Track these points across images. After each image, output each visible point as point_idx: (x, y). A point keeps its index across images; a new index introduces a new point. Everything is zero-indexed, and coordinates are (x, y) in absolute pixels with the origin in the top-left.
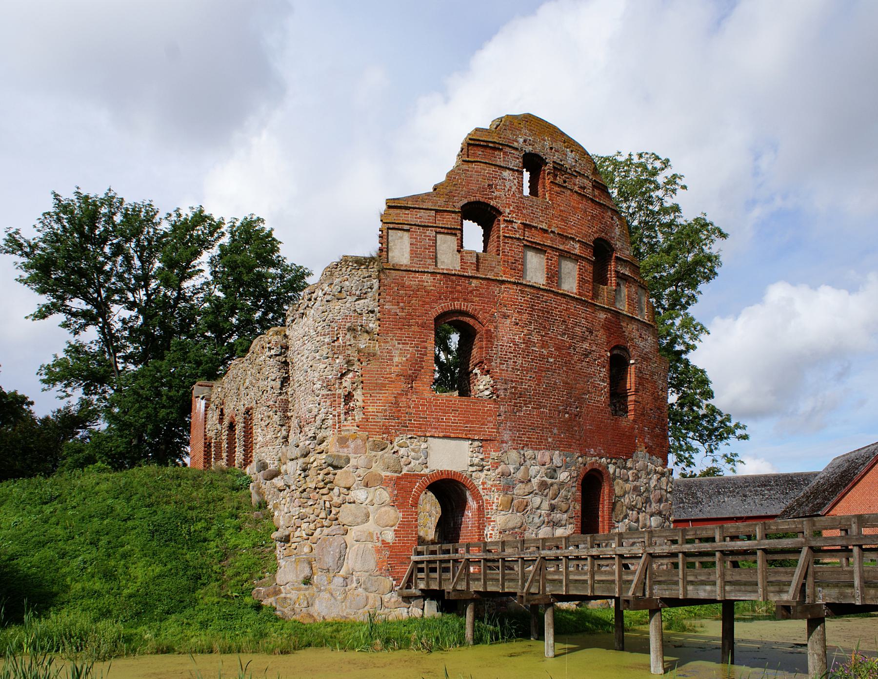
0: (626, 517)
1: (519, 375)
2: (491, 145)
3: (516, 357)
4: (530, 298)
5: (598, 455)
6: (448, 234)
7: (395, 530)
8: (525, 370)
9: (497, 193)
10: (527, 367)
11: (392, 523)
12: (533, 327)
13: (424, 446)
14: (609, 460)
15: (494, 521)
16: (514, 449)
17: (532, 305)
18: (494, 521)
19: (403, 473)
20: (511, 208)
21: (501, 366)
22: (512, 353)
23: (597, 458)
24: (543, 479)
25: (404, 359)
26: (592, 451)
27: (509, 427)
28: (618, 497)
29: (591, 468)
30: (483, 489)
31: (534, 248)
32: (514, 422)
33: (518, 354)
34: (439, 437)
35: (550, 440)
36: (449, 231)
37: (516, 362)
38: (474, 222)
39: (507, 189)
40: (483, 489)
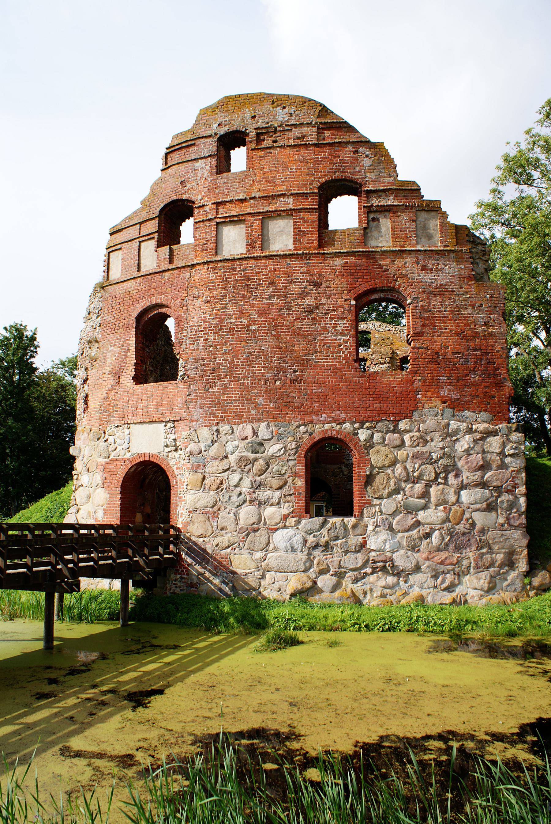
0: (397, 491)
1: (211, 351)
2: (184, 145)
3: (207, 334)
4: (224, 272)
5: (334, 421)
6: (149, 239)
7: (104, 510)
8: (219, 345)
9: (189, 186)
10: (222, 342)
11: (101, 503)
12: (228, 299)
13: (127, 432)
14: (357, 425)
15: (184, 500)
16: (205, 426)
17: (226, 278)
18: (184, 500)
19: (111, 457)
20: (203, 193)
21: (191, 346)
22: (202, 331)
23: (334, 424)
24: (243, 454)
25: (114, 359)
26: (323, 417)
27: (200, 404)
28: (379, 468)
29: (320, 437)
30: (177, 469)
31: (231, 222)
32: (205, 399)
33: (209, 330)
34: (137, 423)
35: (253, 412)
36: (149, 237)
37: (207, 339)
38: (184, 221)
39: (199, 178)
40: (177, 469)
